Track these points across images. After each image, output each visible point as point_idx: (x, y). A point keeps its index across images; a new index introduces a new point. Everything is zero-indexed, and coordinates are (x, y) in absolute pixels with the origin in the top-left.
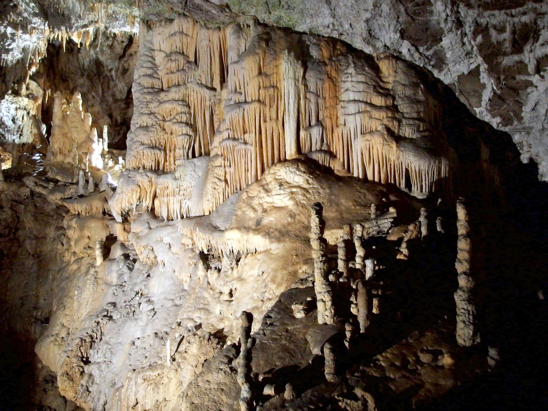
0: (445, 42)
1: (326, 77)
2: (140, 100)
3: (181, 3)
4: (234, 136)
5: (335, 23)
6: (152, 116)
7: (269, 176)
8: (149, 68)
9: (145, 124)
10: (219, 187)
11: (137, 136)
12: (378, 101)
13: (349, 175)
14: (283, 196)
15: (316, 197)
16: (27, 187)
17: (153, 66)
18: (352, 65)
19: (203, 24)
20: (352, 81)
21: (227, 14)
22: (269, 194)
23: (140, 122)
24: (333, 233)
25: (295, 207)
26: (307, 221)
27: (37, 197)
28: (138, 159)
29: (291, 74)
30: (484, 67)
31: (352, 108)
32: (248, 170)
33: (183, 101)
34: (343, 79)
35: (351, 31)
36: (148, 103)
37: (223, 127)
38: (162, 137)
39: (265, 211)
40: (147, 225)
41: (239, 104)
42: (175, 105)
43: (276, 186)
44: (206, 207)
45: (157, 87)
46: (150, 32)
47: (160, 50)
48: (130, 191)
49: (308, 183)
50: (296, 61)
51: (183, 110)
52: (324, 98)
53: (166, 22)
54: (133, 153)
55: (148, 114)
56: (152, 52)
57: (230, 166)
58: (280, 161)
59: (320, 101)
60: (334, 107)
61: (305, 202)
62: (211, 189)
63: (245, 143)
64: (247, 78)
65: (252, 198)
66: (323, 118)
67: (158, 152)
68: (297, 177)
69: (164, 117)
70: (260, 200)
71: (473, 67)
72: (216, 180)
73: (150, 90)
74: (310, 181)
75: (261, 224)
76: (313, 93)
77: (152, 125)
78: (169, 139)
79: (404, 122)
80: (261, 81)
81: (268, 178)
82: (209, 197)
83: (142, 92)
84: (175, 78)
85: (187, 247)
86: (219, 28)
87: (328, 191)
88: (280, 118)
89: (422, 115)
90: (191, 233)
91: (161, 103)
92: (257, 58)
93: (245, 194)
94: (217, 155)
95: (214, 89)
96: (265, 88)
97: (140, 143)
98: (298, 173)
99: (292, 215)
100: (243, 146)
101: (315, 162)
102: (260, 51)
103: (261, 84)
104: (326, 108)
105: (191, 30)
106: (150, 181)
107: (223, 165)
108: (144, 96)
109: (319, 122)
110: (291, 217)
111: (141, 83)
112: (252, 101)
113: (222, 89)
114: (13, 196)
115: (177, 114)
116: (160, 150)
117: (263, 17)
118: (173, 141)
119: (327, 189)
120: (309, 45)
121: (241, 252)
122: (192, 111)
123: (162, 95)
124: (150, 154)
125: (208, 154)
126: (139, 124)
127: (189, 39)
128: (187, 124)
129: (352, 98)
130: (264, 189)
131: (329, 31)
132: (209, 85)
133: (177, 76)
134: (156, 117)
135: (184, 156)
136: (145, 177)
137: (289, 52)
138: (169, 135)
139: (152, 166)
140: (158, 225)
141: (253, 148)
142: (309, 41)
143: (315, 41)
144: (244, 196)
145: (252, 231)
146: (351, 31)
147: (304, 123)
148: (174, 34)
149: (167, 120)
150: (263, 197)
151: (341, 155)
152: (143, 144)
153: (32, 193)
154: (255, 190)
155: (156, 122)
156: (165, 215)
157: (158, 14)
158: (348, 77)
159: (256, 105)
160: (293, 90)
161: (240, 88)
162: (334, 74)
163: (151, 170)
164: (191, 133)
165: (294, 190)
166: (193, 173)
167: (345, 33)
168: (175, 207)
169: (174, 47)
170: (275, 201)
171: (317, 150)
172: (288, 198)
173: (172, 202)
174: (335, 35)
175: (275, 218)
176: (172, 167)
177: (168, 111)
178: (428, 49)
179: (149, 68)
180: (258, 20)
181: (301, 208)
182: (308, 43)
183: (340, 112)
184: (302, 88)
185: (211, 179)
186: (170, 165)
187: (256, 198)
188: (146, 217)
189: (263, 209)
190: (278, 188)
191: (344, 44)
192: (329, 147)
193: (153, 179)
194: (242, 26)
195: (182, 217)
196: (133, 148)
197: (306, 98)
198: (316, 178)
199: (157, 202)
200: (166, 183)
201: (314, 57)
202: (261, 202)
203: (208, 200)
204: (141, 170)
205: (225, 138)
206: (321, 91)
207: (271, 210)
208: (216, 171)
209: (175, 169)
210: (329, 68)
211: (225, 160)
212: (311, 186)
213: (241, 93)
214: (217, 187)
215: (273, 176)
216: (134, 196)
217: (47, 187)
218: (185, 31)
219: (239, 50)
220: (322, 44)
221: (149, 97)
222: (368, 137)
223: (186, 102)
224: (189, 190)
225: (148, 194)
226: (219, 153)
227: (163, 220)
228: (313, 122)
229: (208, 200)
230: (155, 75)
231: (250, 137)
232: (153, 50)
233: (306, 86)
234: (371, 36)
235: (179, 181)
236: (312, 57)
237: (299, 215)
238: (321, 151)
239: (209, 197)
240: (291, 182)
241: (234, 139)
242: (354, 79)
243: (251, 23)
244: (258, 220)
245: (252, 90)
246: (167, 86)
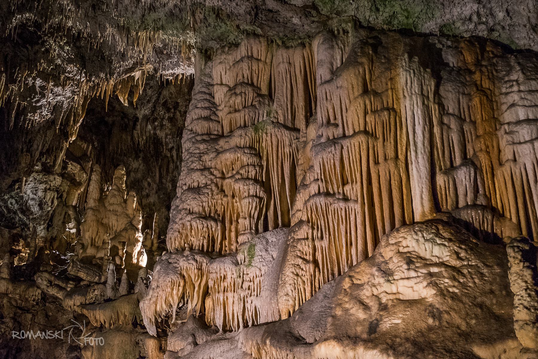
1: (475, 89)
2: (190, 151)
3: (250, 14)
4: (327, 189)
5: (482, 11)
6: (206, 173)
7: (388, 249)
8: (206, 108)
9: (196, 184)
10: (304, 273)
11: (183, 202)
14: (415, 281)
15: (477, 281)
16: (38, 288)
17: (211, 105)
18: (518, 68)
19: (280, 43)
20: (520, 91)
21: (313, 19)
23: (189, 182)
25: (438, 298)
26: (464, 323)
27: (49, 303)
28: (184, 237)
31: (525, 133)
32: (351, 244)
33: (251, 148)
34: (504, 90)
35: (509, 22)
37: (310, 177)
38: (220, 201)
39: (383, 307)
40: (190, 339)
41: (333, 141)
43: (399, 264)
44: (285, 304)
45: (216, 133)
46: (210, 63)
47: (222, 84)
48: (169, 284)
49: (459, 258)
50: (422, 70)
51: (250, 161)
52: (474, 123)
53: (229, 48)
54: (176, 226)
55: (201, 170)
56: (210, 88)
57: (322, 238)
58: (404, 224)
59: (466, 127)
60: (493, 134)
61: (457, 291)
62: (291, 275)
63: (346, 199)
64: (346, 101)
65: (360, 286)
66: (475, 153)
67: (213, 223)
68: (438, 251)
69: (223, 173)
70: (374, 289)
72: (300, 261)
73: (205, 137)
74: (463, 254)
75: (378, 329)
76: (453, 115)
77: (206, 185)
78: (230, 205)
80: (368, 102)
81: (387, 252)
82: (289, 288)
83: (193, 140)
84: (239, 118)
86: (303, 45)
88: (401, 157)
90: (259, 350)
91: (218, 153)
93: (347, 279)
94: (301, 223)
95: (298, 130)
96: (374, 112)
97: (187, 212)
99: (435, 314)
100: (342, 204)
101: (468, 226)
102: (364, 60)
103: (369, 107)
104: (478, 137)
105: (264, 54)
106: (200, 269)
107: (310, 236)
108: (197, 145)
109: (467, 161)
110: (434, 317)
111: (194, 129)
112: (355, 134)
113: (307, 126)
114: (19, 302)
115: (242, 167)
116: (215, 220)
117: (366, 15)
118: (235, 208)
119: (496, 267)
120: (441, 50)
122: (264, 164)
123: (222, 142)
124: (200, 227)
125: (287, 225)
126: (188, 185)
127: (261, 65)
128: (256, 181)
129: (522, 117)
130: (380, 270)
131: (472, 26)
132: (290, 125)
133: (242, 115)
134: (212, 174)
135: (251, 229)
136: (192, 262)
137: (410, 58)
138: (230, 198)
139: (203, 245)
140: (209, 338)
141: (358, 207)
142: (441, 43)
143: (449, 43)
144: (346, 284)
145: (361, 343)
146: (509, 22)
147: (442, 162)
148: (242, 60)
149: (227, 176)
150: (379, 284)
151: (513, 211)
152: (190, 213)
153: (45, 297)
154: (366, 274)
155: (211, 180)
156: (219, 322)
157: (220, 39)
158: (512, 86)
159: (362, 138)
160: (419, 112)
161: (335, 119)
162: (486, 84)
163: (201, 252)
164: (262, 194)
166: (264, 253)
167: (498, 27)
168: (235, 308)
169: (240, 77)
170: (401, 290)
171: (467, 206)
172: (425, 283)
173: (230, 301)
174: (482, 31)
175: (404, 320)
176: (233, 247)
177: (228, 163)
179: (206, 108)
180: (360, 22)
181: (450, 301)
182: (439, 46)
184: (434, 108)
185: (291, 260)
186: (230, 244)
187: (366, 286)
188: (190, 325)
190: (405, 266)
191: (496, 43)
192: (489, 199)
193: (204, 265)
194: (336, 32)
195: (246, 326)
196: (177, 220)
197: (441, 123)
198: (472, 249)
199: (209, 303)
200: (222, 271)
201: (451, 65)
203: (287, 295)
204: (187, 253)
205: (313, 193)
207: (394, 306)
208: (299, 247)
209: (237, 250)
210: (477, 76)
211: (313, 229)
212: (465, 263)
213: (337, 125)
214: (301, 273)
215: (393, 248)
216: (175, 292)
217: (64, 289)
218: (255, 55)
219: (332, 64)
220: (462, 45)
221: (202, 147)
223: (255, 150)
224: (257, 281)
225: (196, 289)
226: (305, 218)
227: (217, 331)
228: (458, 161)
229: (287, 295)
230: (213, 117)
231: (353, 190)
232: (213, 85)
233: (441, 105)
235: (242, 266)
236: (447, 65)
237: (448, 313)
238: (474, 206)
239: (289, 288)
240: (428, 257)
241: (327, 194)
242: (522, 88)
243: (349, 27)
244: (371, 323)
245: (354, 118)
246: (228, 130)
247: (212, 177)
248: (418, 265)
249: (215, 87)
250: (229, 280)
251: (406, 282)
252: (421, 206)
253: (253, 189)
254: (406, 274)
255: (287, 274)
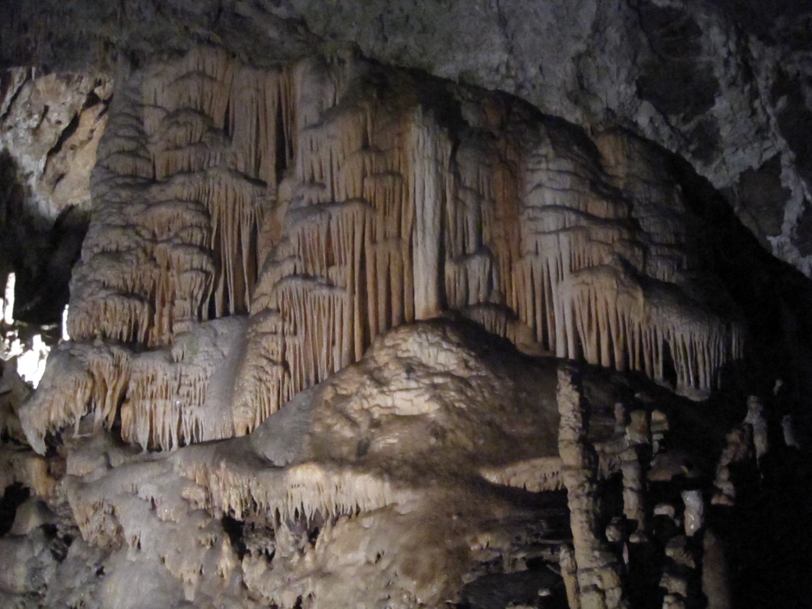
0: (721, 106)
1: (498, 160)
2: (106, 198)
3: (208, 14)
4: (306, 270)
5: (512, 63)
6: (130, 232)
7: (383, 353)
8: (130, 138)
9: (113, 247)
10: (269, 378)
11: (95, 271)
12: (601, 208)
13: (548, 354)
14: (415, 393)
15: (486, 395)
17: (137, 135)
18: (548, 141)
19: (246, 59)
20: (548, 169)
21: (299, 37)
22: (385, 389)
23: (103, 242)
24: (534, 467)
25: (442, 414)
26: (470, 444)
28: (94, 319)
29: (429, 151)
30: (788, 157)
31: (551, 221)
32: (333, 343)
34: (530, 166)
35: (540, 80)
36: (123, 204)
37: (283, 252)
38: (148, 273)
39: (375, 424)
40: (102, 459)
41: (319, 207)
42: (180, 210)
43: (397, 372)
44: (241, 418)
45: (144, 175)
46: (138, 74)
47: (155, 106)
48: (72, 385)
49: (467, 366)
50: (437, 127)
51: (195, 221)
52: (493, 202)
53: (170, 56)
54: (83, 304)
56: (138, 109)
57: (295, 333)
58: (403, 322)
59: (484, 207)
60: (514, 218)
61: (463, 406)
62: (253, 380)
63: (330, 285)
64: (338, 156)
65: (346, 398)
66: (492, 240)
67: (138, 303)
68: (444, 357)
69: (154, 234)
70: (365, 402)
71: (769, 155)
72: (264, 362)
73: (128, 180)
74: (472, 363)
75: (369, 450)
76: (471, 189)
77: (129, 249)
78: (163, 279)
79: (653, 250)
80: (367, 161)
81: (381, 356)
82: (248, 397)
84: (182, 158)
85: (193, 507)
86: (279, 68)
87: (510, 383)
88: (405, 236)
89: (683, 240)
90: (206, 475)
91: (149, 205)
92: (361, 119)
93: (329, 389)
94: (267, 311)
95: (263, 184)
96: (376, 175)
97: (101, 285)
98: (445, 345)
99: (438, 432)
100: (325, 292)
101: (478, 328)
102: (366, 105)
103: (368, 169)
104: (497, 219)
105: (220, 71)
106: (117, 366)
107: (280, 330)
109: (482, 249)
111: (112, 167)
112: (348, 201)
113: (279, 179)
115: (184, 228)
116: (142, 300)
117: (370, 45)
118: (171, 284)
119: (508, 379)
120: (458, 103)
121: (323, 514)
122: (214, 226)
123: (155, 190)
124: (119, 307)
125: (242, 311)
126: (101, 247)
127: (216, 87)
128: (202, 249)
129: (549, 202)
130: (372, 378)
131: (498, 78)
132: (252, 175)
133: (186, 155)
134: (138, 233)
135: (192, 313)
136: (107, 355)
137: (425, 111)
138: (163, 270)
139: (121, 333)
140: (128, 459)
141: (345, 296)
142: (460, 94)
143: (470, 96)
144: (328, 394)
145: (349, 466)
146: (540, 80)
148: (188, 75)
149: (159, 239)
150: (371, 395)
151: (530, 313)
152: (105, 286)
154: (351, 383)
155: (137, 242)
156: (143, 439)
157: (158, 40)
158: (539, 162)
159: (357, 208)
160: (432, 183)
161: (321, 177)
162: (511, 156)
163: (119, 342)
164: (209, 268)
165: (439, 380)
166: (211, 349)
167: (528, 85)
168: (166, 422)
169: (185, 100)
170: (398, 403)
171: (478, 305)
172: (427, 396)
173: (160, 410)
174: (509, 87)
175: (401, 440)
176: (165, 338)
177: (164, 220)
178: (686, 120)
179: (130, 138)
180: (361, 52)
181: (456, 418)
182: (458, 98)
183: (527, 229)
184: (449, 179)
185: (252, 360)
186: (160, 332)
187: (355, 398)
188: (101, 442)
189: (372, 420)
190: (404, 375)
191: (526, 105)
192: (503, 296)
193: (123, 361)
194: (329, 60)
195: (182, 444)
197: (456, 198)
198: (483, 356)
199: (126, 412)
200: (151, 371)
201: (471, 124)
202: (366, 406)
203: (245, 405)
204: (98, 342)
205: (286, 273)
206: (486, 188)
207: (389, 423)
208: (264, 343)
209: (170, 342)
210: (501, 144)
211: (284, 320)
212: (474, 373)
213: (322, 186)
214: (264, 377)
215: (391, 351)
216: (79, 395)
218: (209, 71)
219: (321, 103)
220: (485, 101)
221: (124, 194)
222: (586, 277)
223: (203, 205)
224: (199, 385)
225: (109, 393)
226: (273, 306)
227: (139, 449)
228: (472, 247)
229: (245, 405)
230: (141, 153)
231: (341, 274)
232: (142, 106)
233: (457, 176)
234: (581, 92)
235: (179, 365)
236: (466, 123)
237: (452, 431)
238: (487, 304)
239: (248, 397)
240: (431, 363)
241: (306, 277)
242: (551, 166)
243: (347, 55)
244: (360, 443)
245: (347, 179)
246: (164, 174)
247: (138, 238)
248: (419, 374)
249: (146, 110)
250: (159, 382)
251: (404, 394)
252: (424, 300)
253: (201, 260)
254: (405, 384)
255: (246, 377)
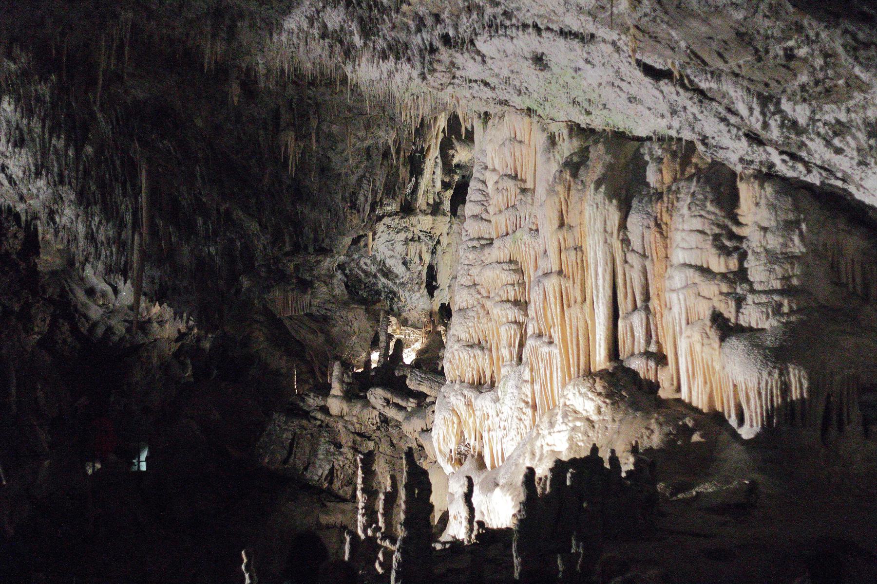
6: (472, 291)
12: (718, 264)
13: (677, 396)
16: (374, 408)
17: (483, 198)
27: (392, 427)
29: (599, 225)
33: (511, 261)
49: (599, 412)
50: (607, 202)
55: (469, 287)
79: (750, 298)
89: (795, 282)
92: (557, 201)
98: (590, 395)
114: (357, 426)
120: (647, 163)
124: (467, 357)
147: (624, 306)
153: (385, 420)
166: (515, 391)
184: (617, 244)
206: (653, 247)
214: (523, 417)
217: (405, 408)
233: (626, 241)
236: (647, 185)
